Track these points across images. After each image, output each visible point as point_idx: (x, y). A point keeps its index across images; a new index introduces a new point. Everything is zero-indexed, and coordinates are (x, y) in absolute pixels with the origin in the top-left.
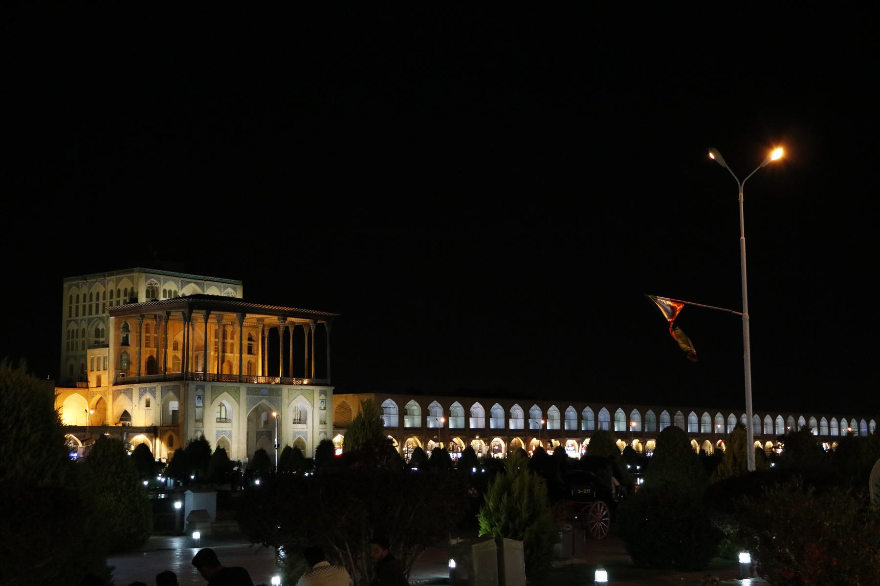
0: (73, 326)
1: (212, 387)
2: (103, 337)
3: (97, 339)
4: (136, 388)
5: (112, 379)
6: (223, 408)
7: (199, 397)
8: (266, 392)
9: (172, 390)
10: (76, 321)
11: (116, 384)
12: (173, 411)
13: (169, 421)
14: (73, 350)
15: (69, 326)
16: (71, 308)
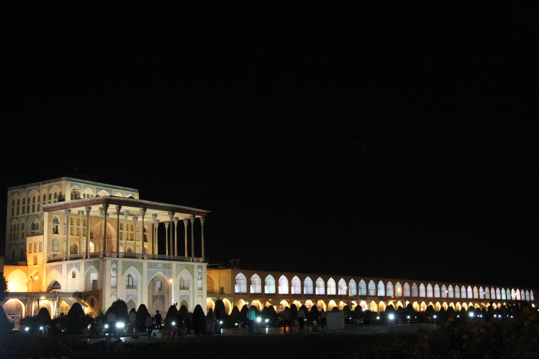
0: (15, 222)
1: (123, 262)
2: (37, 229)
3: (33, 231)
4: (64, 264)
5: (46, 259)
6: (130, 278)
7: (114, 270)
8: (161, 266)
9: (94, 264)
10: (17, 218)
11: (49, 262)
12: (94, 281)
13: (90, 288)
14: (14, 239)
15: (12, 222)
16: (13, 209)
